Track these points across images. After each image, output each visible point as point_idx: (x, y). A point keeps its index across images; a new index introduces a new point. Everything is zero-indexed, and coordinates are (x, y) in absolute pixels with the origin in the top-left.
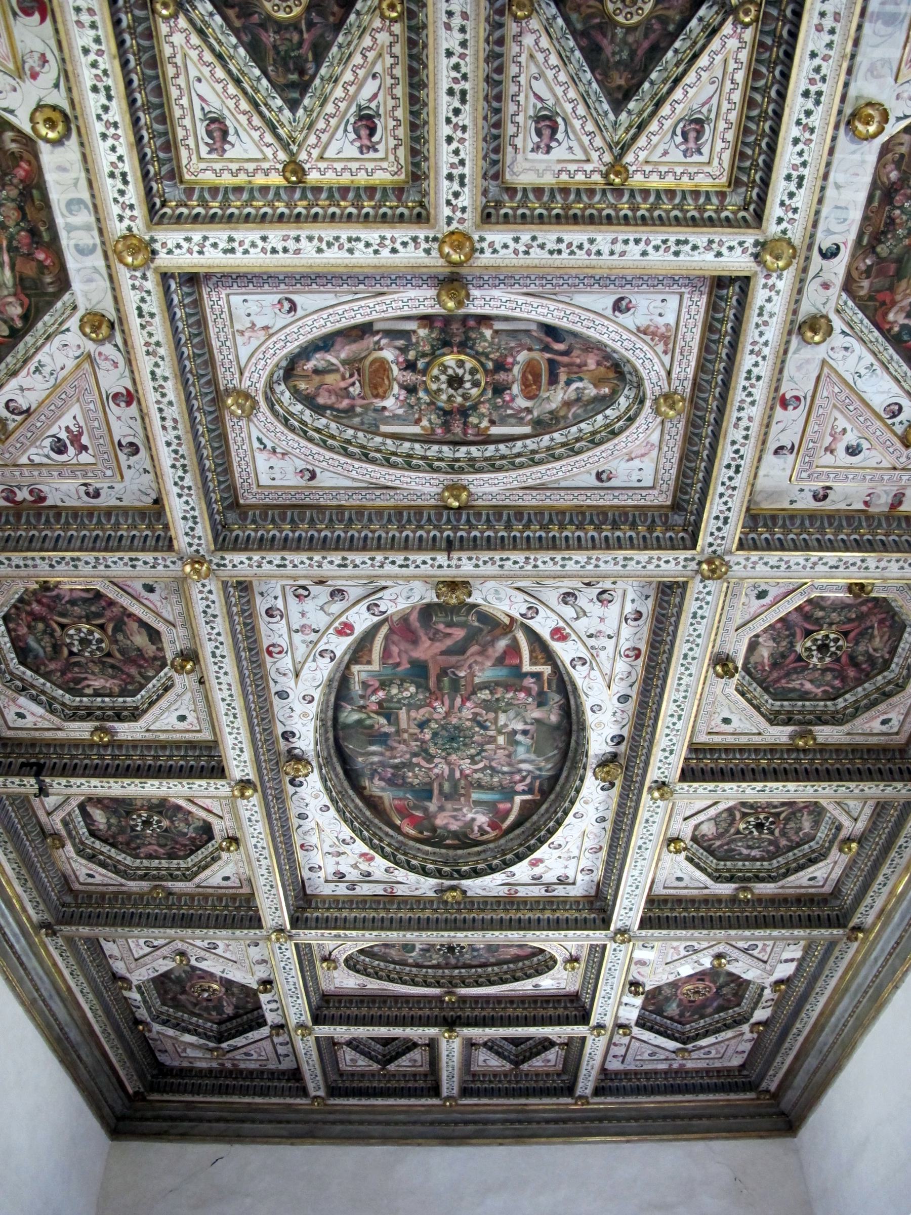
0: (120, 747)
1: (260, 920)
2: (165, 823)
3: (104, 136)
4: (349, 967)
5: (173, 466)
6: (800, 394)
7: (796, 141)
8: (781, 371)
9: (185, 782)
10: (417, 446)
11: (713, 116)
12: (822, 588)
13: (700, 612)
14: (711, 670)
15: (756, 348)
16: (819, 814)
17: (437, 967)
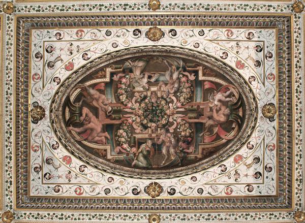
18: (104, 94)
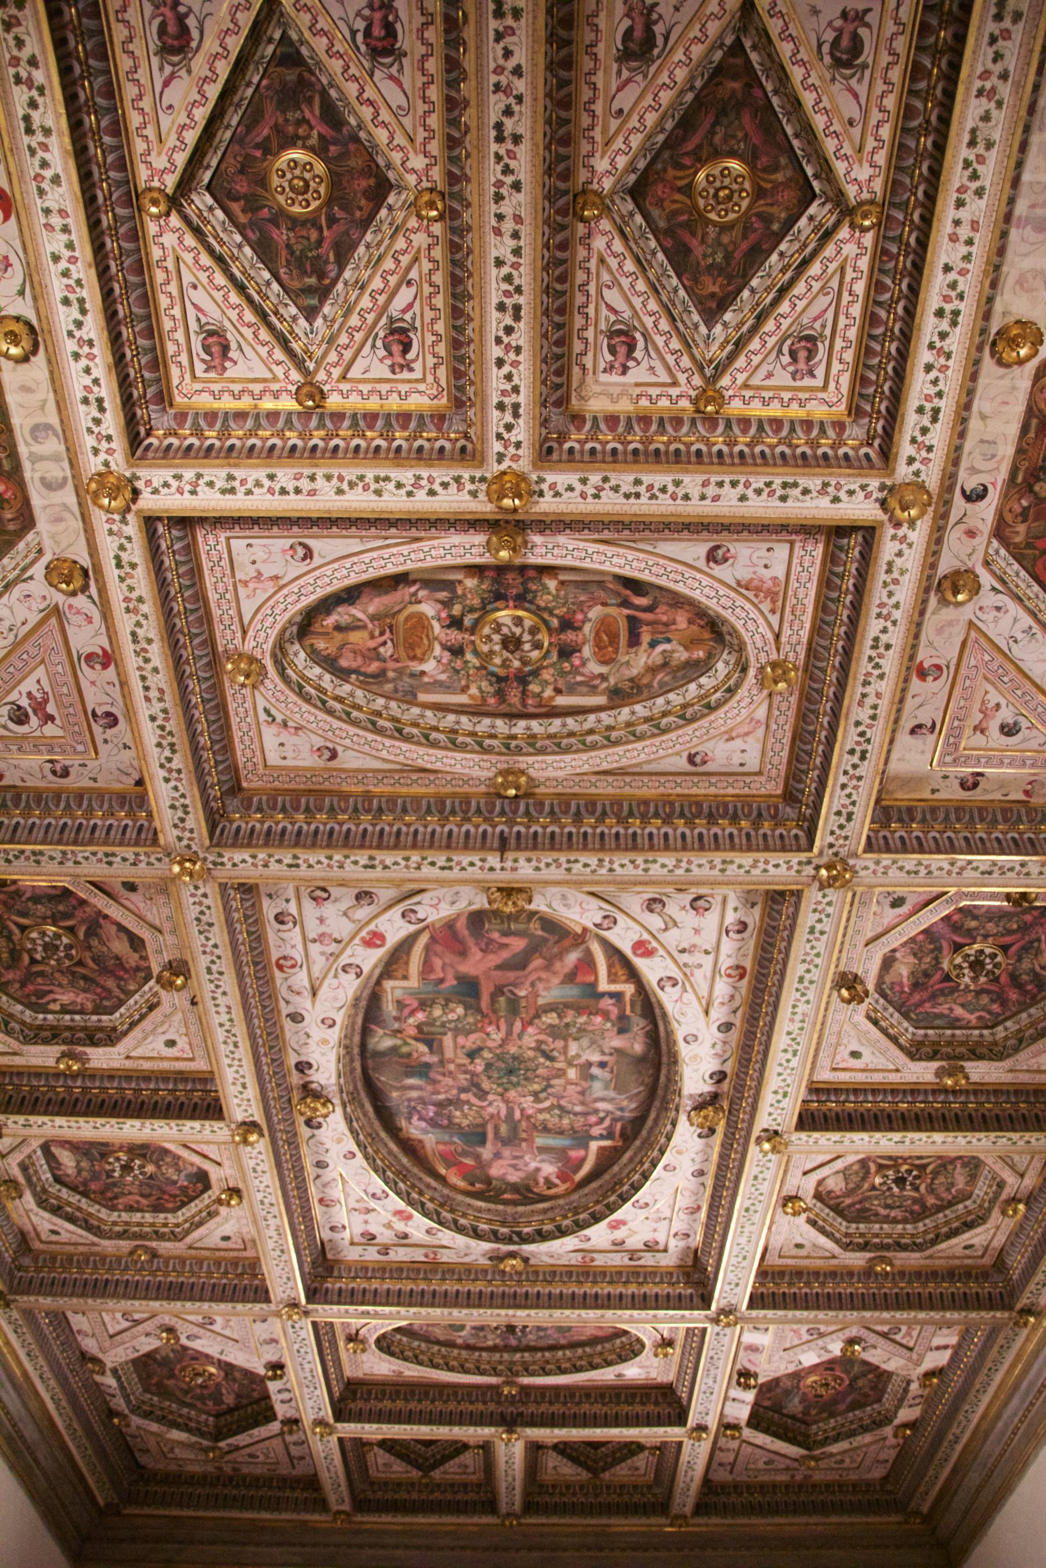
0: (93, 1077)
1: (267, 1292)
2: (150, 1169)
3: (76, 356)
4: (381, 1349)
5: (159, 745)
6: (942, 662)
7: (929, 368)
8: (917, 636)
9: (173, 1123)
10: (464, 719)
11: (828, 332)
12: (974, 896)
13: (819, 927)
14: (835, 994)
15: (885, 611)
16: (977, 1167)
17: (494, 1349)
18: (562, 983)
